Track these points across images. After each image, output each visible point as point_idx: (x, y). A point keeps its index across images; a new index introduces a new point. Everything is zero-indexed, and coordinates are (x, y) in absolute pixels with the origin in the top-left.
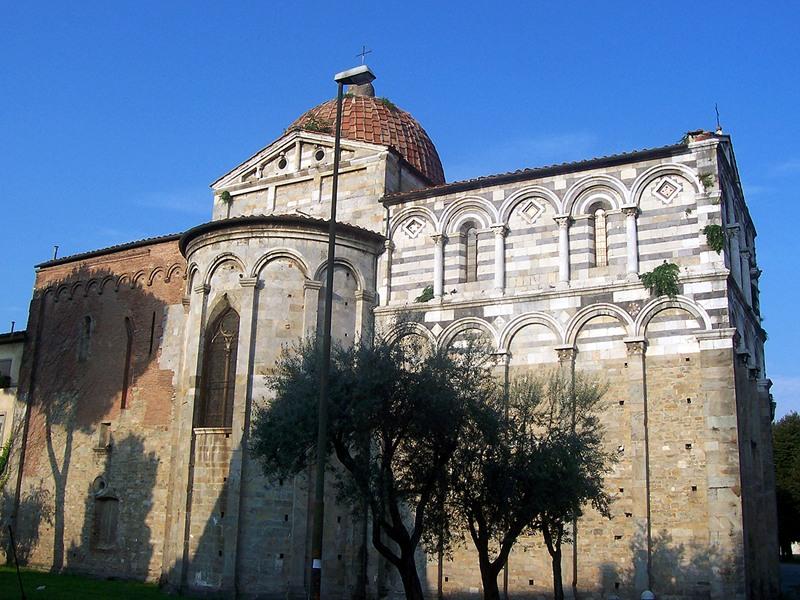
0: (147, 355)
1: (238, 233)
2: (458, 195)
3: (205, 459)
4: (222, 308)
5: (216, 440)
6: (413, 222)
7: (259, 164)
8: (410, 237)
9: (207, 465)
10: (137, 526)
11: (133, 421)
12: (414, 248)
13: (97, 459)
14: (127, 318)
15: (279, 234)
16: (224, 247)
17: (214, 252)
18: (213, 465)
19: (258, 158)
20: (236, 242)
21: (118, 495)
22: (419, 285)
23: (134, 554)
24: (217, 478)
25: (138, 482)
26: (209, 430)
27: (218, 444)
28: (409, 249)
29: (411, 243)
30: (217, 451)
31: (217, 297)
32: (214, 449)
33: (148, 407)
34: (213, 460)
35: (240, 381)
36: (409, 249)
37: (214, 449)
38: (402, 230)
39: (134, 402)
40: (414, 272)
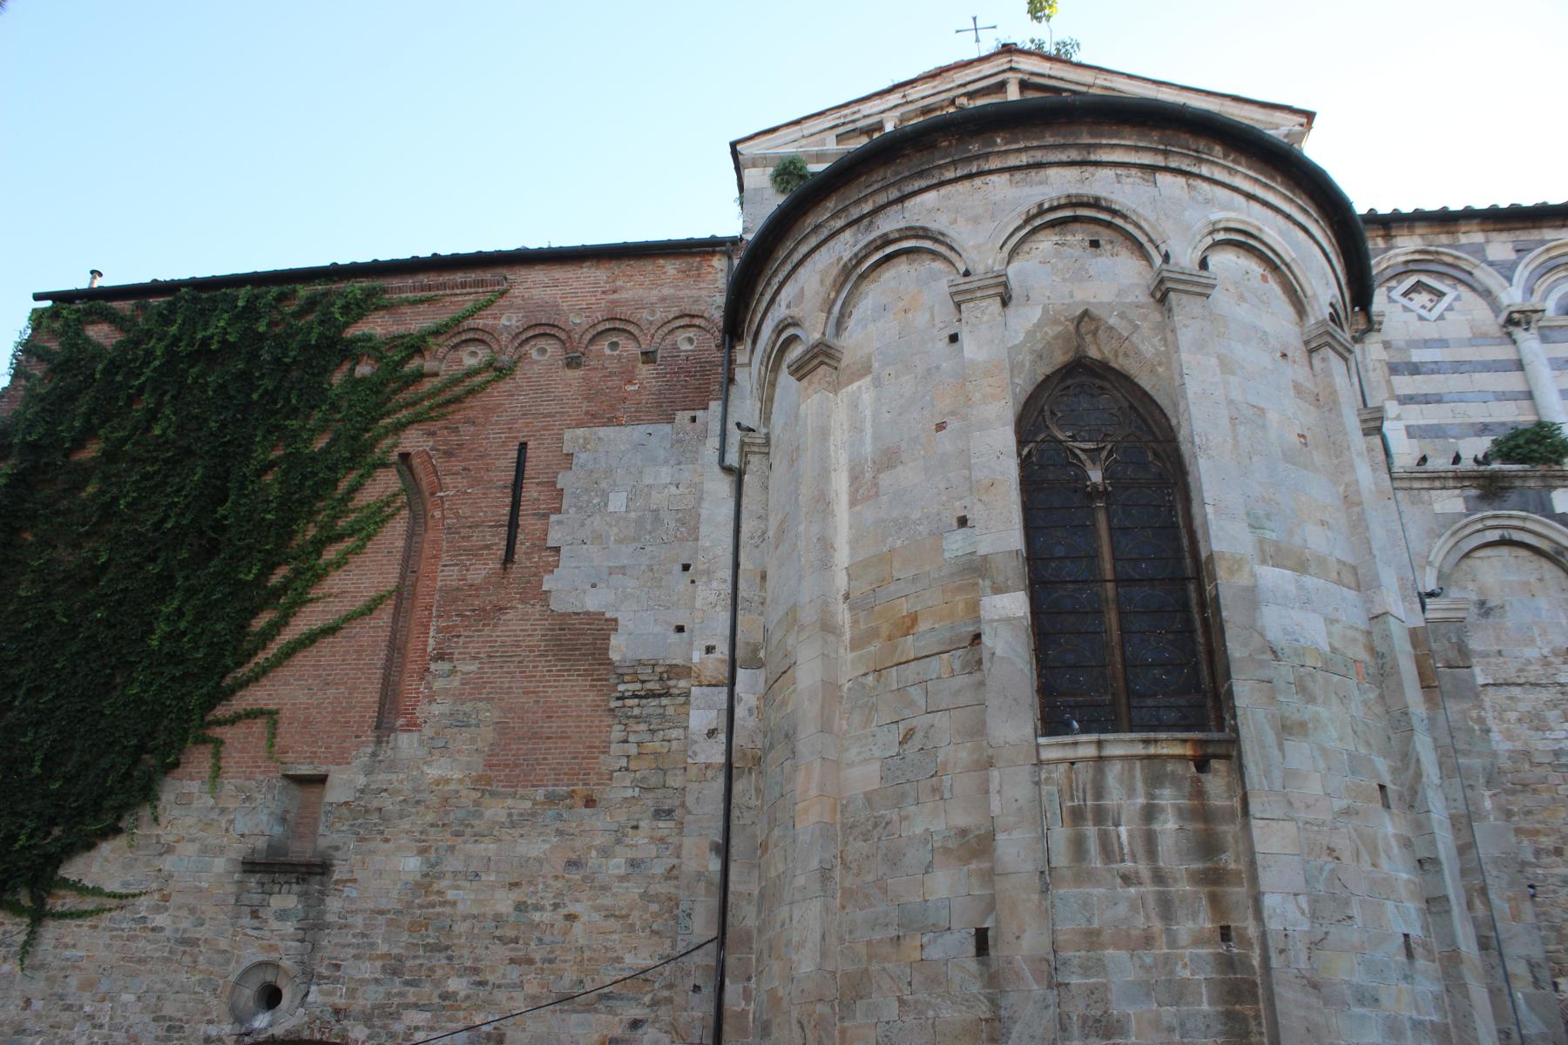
0: (494, 565)
1: (1120, 148)
2: (1549, 234)
3: (1107, 852)
4: (1060, 358)
5: (1155, 781)
6: (1418, 287)
7: (897, 113)
8: (1421, 318)
9: (1127, 879)
11: (433, 772)
12: (1442, 343)
13: (256, 898)
15: (1238, 182)
16: (1060, 183)
17: (1027, 190)
18: (1159, 877)
19: (895, 99)
20: (1108, 173)
22: (1484, 429)
24: (1185, 928)
25: (456, 984)
26: (1121, 745)
27: (1168, 798)
28: (1426, 344)
29: (1430, 331)
30: (1168, 825)
31: (1048, 319)
32: (1150, 813)
33: (501, 728)
35: (1231, 572)
36: (1426, 344)
37: (1150, 813)
38: (1391, 300)
39: (436, 709)
40: (1461, 398)
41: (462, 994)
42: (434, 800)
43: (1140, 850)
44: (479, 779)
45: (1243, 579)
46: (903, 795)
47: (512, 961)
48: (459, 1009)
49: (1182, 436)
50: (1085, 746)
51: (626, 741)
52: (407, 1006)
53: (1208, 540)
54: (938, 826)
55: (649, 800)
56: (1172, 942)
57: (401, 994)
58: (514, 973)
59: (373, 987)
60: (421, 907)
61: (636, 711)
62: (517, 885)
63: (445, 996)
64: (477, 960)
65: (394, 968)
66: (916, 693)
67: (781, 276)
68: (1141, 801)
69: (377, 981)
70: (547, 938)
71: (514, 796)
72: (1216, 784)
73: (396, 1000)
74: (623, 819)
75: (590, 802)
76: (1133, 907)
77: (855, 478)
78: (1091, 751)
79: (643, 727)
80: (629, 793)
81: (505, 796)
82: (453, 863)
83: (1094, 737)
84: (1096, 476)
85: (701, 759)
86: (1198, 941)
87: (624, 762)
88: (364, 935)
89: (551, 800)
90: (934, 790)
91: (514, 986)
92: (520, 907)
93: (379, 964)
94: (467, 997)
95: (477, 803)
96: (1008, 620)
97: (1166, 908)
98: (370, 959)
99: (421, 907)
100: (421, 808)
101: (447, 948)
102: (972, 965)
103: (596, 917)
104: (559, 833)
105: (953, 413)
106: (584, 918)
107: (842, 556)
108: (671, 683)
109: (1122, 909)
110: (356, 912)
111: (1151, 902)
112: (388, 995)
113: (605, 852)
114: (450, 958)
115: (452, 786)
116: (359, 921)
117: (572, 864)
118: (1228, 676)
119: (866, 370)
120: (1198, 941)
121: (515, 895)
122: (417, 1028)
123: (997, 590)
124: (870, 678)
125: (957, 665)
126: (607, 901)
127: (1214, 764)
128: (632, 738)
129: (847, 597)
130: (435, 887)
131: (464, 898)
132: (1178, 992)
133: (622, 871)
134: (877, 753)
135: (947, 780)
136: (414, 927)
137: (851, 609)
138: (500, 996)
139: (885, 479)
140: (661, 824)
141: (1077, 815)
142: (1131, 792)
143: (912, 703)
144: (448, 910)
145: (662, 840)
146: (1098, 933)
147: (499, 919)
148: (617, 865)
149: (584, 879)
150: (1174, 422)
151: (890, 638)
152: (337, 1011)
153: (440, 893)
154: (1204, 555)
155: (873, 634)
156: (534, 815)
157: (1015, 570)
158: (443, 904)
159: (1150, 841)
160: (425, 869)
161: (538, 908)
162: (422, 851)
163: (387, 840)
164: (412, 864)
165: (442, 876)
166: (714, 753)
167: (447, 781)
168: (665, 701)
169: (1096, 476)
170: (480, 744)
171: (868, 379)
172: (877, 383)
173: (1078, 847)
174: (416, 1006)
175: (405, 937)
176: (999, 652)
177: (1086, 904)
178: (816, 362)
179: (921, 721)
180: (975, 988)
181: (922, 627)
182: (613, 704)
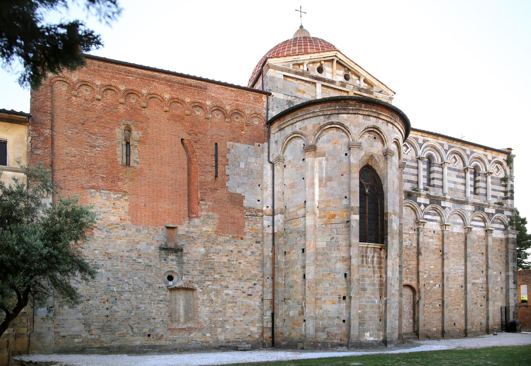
3: (367, 263)
5: (374, 252)
10: (221, 309)
11: (204, 229)
14: (182, 140)
18: (373, 267)
21: (196, 286)
23: (219, 330)
24: (376, 275)
25: (216, 276)
26: (372, 245)
27: (376, 255)
30: (375, 259)
32: (373, 257)
34: (373, 263)
37: (373, 257)
41: (218, 278)
42: (206, 235)
43: (371, 263)
44: (216, 231)
45: (391, 218)
46: (331, 249)
47: (228, 272)
48: (218, 281)
49: (384, 186)
50: (365, 244)
51: (249, 226)
52: (206, 281)
53: (387, 209)
54: (338, 255)
55: (254, 239)
56: (374, 278)
57: (204, 278)
58: (229, 274)
59: (197, 276)
60: (206, 259)
61: (250, 219)
62: (227, 256)
63: (214, 278)
64: (220, 271)
65: (202, 273)
66: (335, 230)
67: (298, 119)
68: (372, 255)
69: (198, 275)
70: (235, 267)
71: (225, 236)
72: (382, 253)
73: (204, 279)
74: (249, 243)
75: (242, 239)
76: (370, 272)
77: (320, 181)
78: (366, 246)
79: (252, 223)
80: (250, 237)
81: (223, 236)
82: (212, 250)
83: (367, 243)
84: (367, 191)
85: (267, 232)
86: (378, 277)
87: (249, 230)
88: (193, 265)
89: (233, 237)
90: (338, 249)
91: (229, 277)
92: (229, 260)
93: (198, 271)
94: (219, 279)
95: (216, 237)
96: (356, 220)
97: (374, 272)
98: (196, 270)
99: (206, 259)
100: (203, 237)
101: (213, 269)
102: (344, 279)
103: (245, 263)
104: (236, 245)
105: (345, 173)
106: (243, 263)
107: (317, 198)
108: (258, 213)
109: (368, 272)
110: (191, 260)
111: (372, 271)
112: (202, 278)
113: (246, 250)
114: (214, 271)
115: (210, 233)
116: (192, 262)
117: (239, 252)
118: (387, 235)
119: (324, 155)
120: (378, 277)
121: (227, 258)
122: (209, 285)
123: (355, 214)
124: (324, 225)
125: (343, 226)
126: (247, 260)
127: (382, 249)
128: (250, 225)
129: (318, 207)
130: (209, 255)
131: (216, 258)
132: (374, 285)
133: (250, 254)
134: (325, 240)
135: (340, 248)
136: (205, 264)
137: (319, 210)
138: (227, 278)
139: (329, 183)
140: (257, 245)
141: (363, 256)
142: (371, 253)
143: (333, 232)
144: (213, 260)
145: (258, 248)
146: (364, 275)
147: (224, 263)
148: (249, 253)
149: (242, 255)
150: (383, 183)
151: (329, 218)
152: (190, 282)
153: (210, 257)
154: (385, 212)
155: (325, 217)
156: (230, 240)
157: (357, 210)
158: (212, 259)
159: (373, 261)
160: (206, 251)
161: (232, 261)
162: (205, 247)
163: (196, 244)
164: (203, 250)
165: (210, 253)
166: (270, 230)
167: (208, 231)
168: (257, 217)
169: (367, 191)
170: (215, 223)
171: (325, 158)
172: (327, 159)
173: (363, 261)
174: (208, 280)
175: (204, 266)
176: (354, 226)
177: (363, 271)
178: (312, 150)
179: (336, 236)
180: (344, 283)
181: (337, 217)
182: (245, 217)
